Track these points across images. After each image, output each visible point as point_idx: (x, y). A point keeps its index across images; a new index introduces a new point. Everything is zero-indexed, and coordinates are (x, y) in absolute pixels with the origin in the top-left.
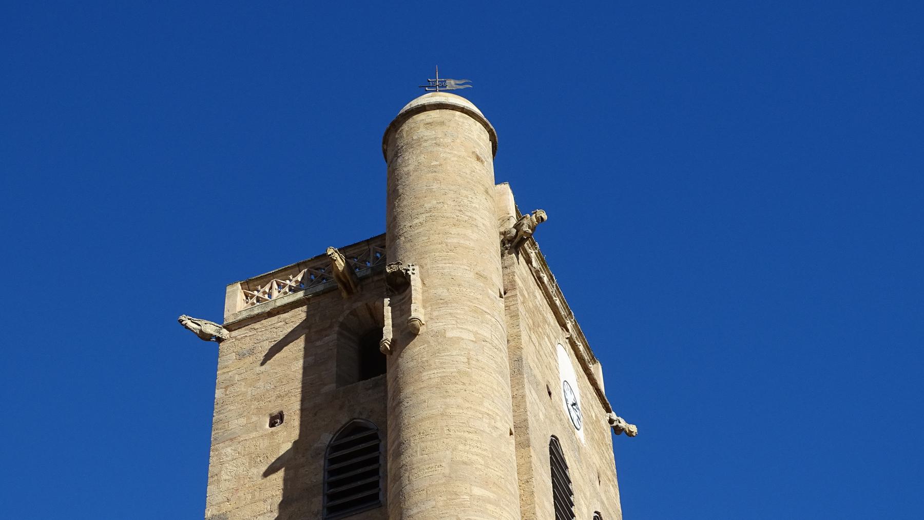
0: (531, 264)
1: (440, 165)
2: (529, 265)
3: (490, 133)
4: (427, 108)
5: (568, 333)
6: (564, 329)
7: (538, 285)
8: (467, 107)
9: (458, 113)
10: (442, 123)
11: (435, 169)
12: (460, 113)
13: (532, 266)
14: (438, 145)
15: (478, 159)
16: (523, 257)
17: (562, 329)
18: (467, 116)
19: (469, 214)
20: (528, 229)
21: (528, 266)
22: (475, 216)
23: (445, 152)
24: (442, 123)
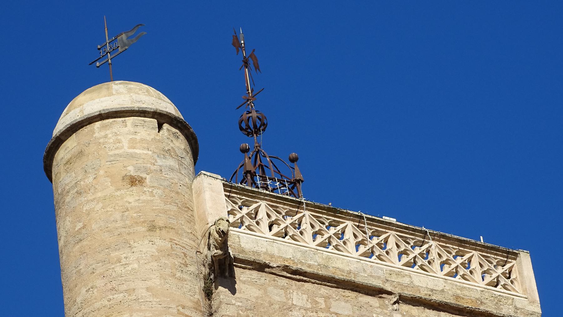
0: (269, 267)
1: (84, 227)
2: (267, 270)
3: (156, 116)
4: (63, 138)
5: (393, 296)
6: (384, 296)
7: (299, 280)
8: (104, 110)
9: (98, 124)
10: (81, 154)
11: (80, 236)
12: (100, 122)
13: (272, 268)
14: (79, 193)
15: (134, 181)
16: (249, 269)
17: (380, 297)
18: (111, 120)
19: (124, 287)
20: (216, 251)
21: (266, 272)
22: (132, 285)
23: (88, 201)
24: (81, 154)
